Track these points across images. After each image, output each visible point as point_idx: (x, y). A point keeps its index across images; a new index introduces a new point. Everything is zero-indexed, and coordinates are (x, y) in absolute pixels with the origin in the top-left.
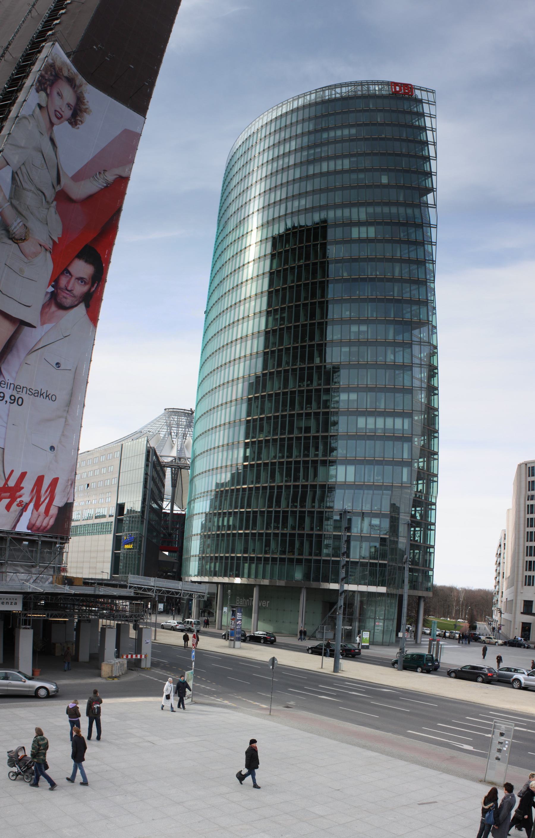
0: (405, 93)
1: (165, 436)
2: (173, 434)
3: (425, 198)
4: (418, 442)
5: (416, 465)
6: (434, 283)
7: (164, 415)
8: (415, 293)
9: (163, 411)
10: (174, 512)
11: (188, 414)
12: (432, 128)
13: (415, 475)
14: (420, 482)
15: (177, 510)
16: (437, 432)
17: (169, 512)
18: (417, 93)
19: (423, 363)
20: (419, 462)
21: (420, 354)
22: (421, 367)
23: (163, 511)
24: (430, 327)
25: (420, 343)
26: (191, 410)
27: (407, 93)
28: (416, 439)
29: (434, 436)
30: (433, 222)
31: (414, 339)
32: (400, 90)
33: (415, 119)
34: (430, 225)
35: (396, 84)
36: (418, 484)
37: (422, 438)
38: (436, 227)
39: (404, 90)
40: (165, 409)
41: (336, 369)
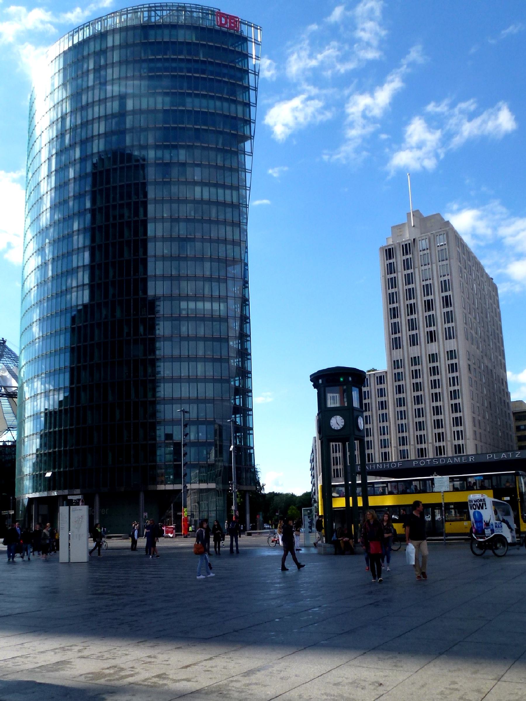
0: (231, 28)
3: (242, 144)
4: (234, 362)
5: (232, 383)
6: (247, 225)
8: (229, 233)
12: (255, 72)
13: (232, 392)
14: (237, 397)
16: (250, 354)
18: (244, 28)
20: (235, 381)
21: (235, 289)
27: (232, 28)
28: (232, 361)
29: (247, 358)
30: (248, 166)
31: (229, 275)
32: (226, 22)
33: (238, 59)
34: (245, 170)
35: (222, 15)
36: (235, 399)
37: (237, 360)
38: (251, 173)
39: (231, 23)
41: (156, 299)
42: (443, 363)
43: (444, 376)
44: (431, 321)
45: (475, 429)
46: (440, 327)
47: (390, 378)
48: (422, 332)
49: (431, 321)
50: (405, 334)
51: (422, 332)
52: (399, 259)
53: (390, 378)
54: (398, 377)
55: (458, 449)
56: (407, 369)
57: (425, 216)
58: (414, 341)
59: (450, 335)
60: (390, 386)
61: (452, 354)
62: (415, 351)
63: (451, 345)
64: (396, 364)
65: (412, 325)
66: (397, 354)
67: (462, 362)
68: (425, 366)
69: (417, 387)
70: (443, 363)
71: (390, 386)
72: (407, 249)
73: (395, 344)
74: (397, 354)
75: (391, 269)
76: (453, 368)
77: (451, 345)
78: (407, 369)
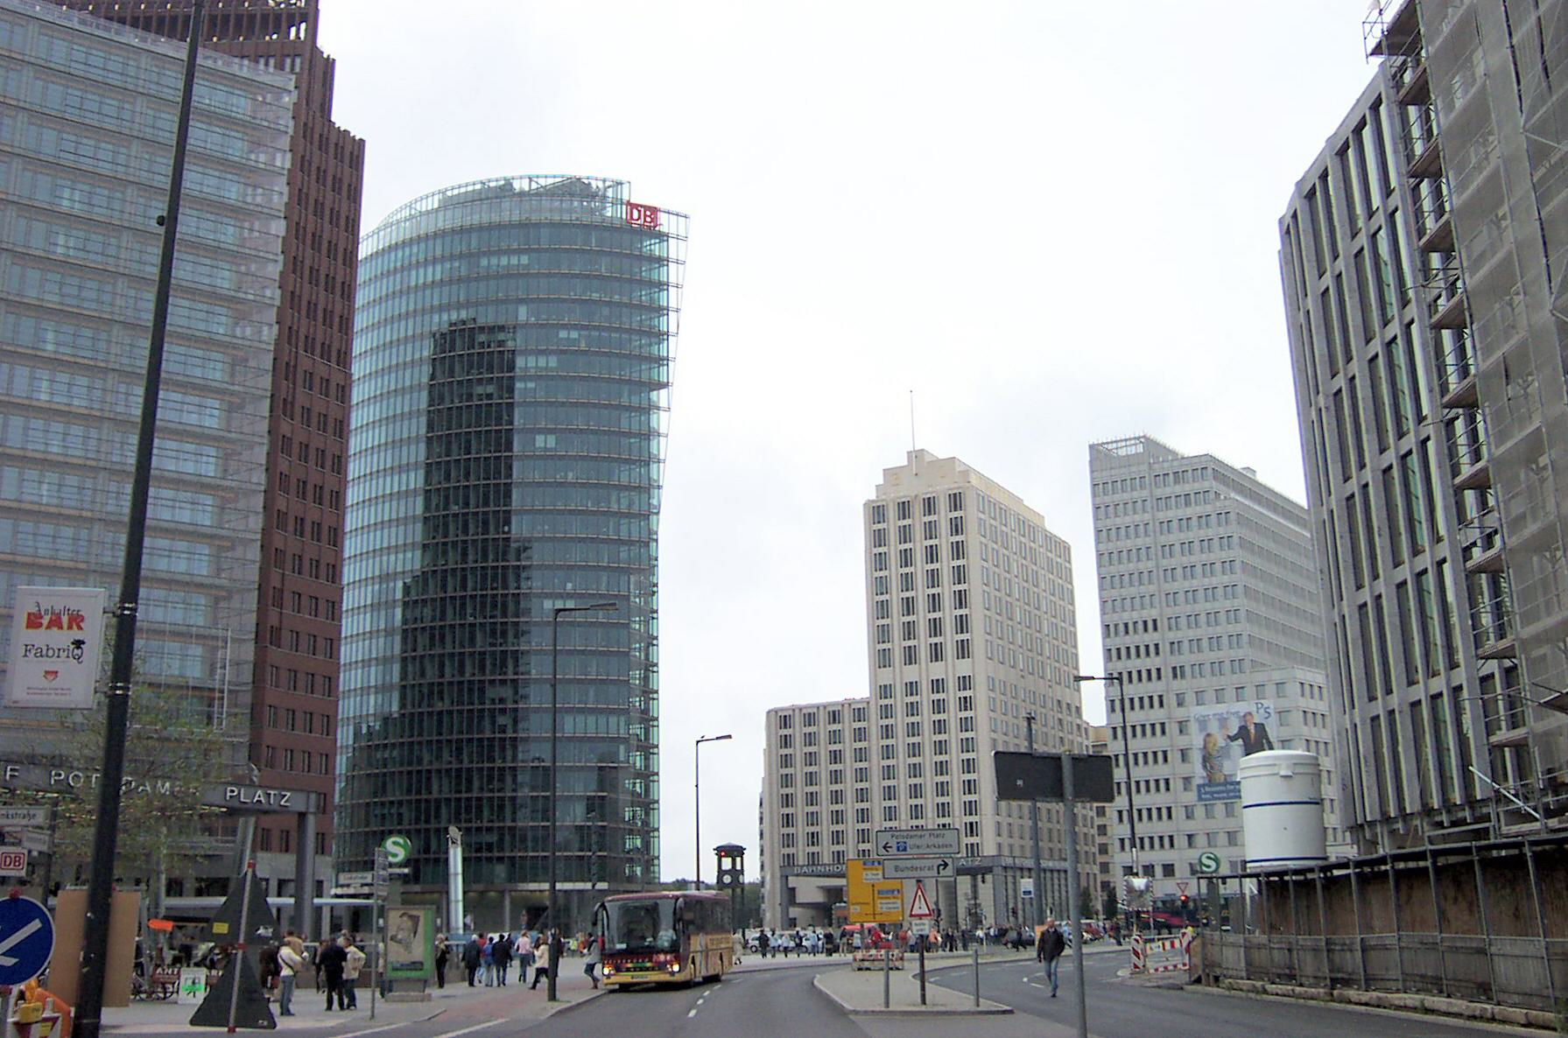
42: (952, 695)
43: (953, 715)
46: (949, 638)
47: (874, 713)
48: (923, 641)
49: (936, 627)
50: (897, 645)
51: (923, 641)
52: (893, 524)
53: (874, 713)
54: (887, 712)
56: (899, 701)
58: (910, 657)
60: (874, 724)
61: (965, 683)
62: (911, 674)
63: (964, 667)
64: (885, 691)
65: (909, 631)
66: (886, 676)
67: (980, 694)
68: (926, 697)
69: (862, 795)
70: (952, 695)
71: (874, 724)
72: (904, 509)
73: (882, 659)
74: (886, 676)
75: (878, 538)
76: (966, 703)
77: (964, 667)
78: (899, 701)
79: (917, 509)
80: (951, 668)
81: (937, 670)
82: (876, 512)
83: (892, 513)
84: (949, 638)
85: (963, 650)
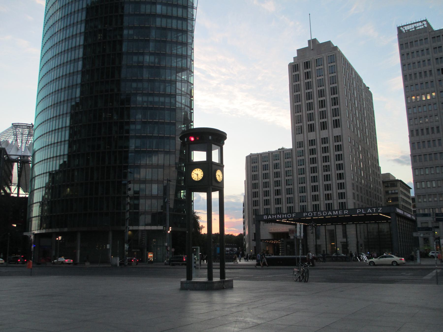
1: (13, 142)
2: (18, 141)
7: (12, 128)
9: (11, 125)
10: (20, 196)
11: (30, 127)
15: (22, 194)
17: (16, 195)
19: (183, 93)
22: (181, 96)
23: (12, 195)
24: (188, 71)
25: (182, 81)
26: (32, 125)
31: (178, 78)
40: (13, 124)
42: (331, 144)
43: (332, 153)
44: (323, 115)
45: (354, 191)
46: (330, 120)
48: (317, 122)
49: (323, 115)
50: (305, 124)
51: (317, 122)
52: (302, 71)
55: (343, 206)
57: (320, 42)
59: (337, 124)
61: (338, 138)
63: (337, 132)
64: (298, 144)
67: (346, 144)
68: (319, 146)
70: (331, 144)
72: (307, 65)
74: (300, 138)
77: (337, 132)
78: (307, 148)
79: (313, 64)
80: (331, 132)
81: (324, 134)
82: (294, 68)
83: (301, 67)
84: (330, 120)
85: (337, 124)
